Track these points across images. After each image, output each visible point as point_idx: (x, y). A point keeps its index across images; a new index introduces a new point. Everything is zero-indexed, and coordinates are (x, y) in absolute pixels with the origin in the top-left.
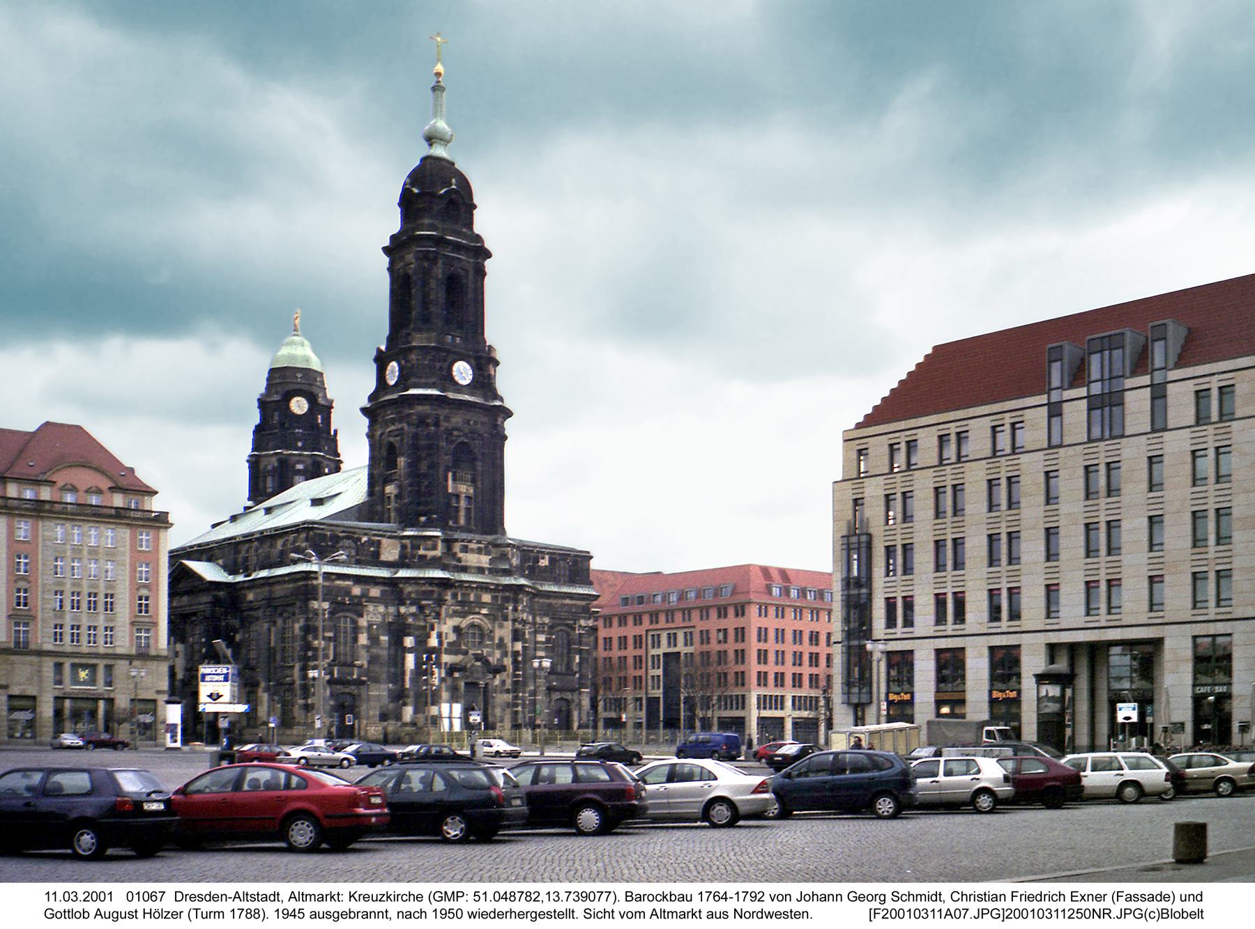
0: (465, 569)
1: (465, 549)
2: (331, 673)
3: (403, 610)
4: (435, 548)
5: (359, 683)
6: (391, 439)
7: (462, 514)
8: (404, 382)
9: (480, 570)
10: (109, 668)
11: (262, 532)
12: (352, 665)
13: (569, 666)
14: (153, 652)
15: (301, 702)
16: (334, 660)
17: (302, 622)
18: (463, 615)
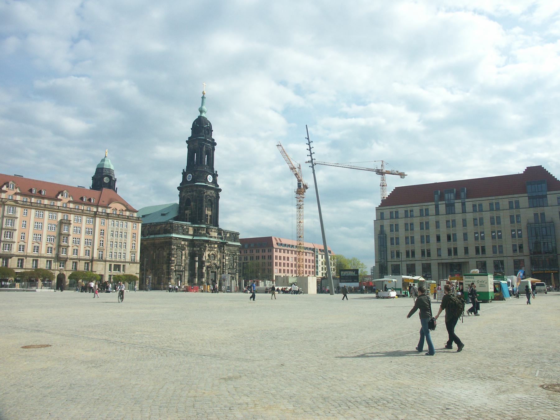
0: (211, 237)
1: (211, 231)
2: (176, 268)
3: (195, 249)
4: (204, 231)
5: (182, 271)
6: (189, 197)
7: (209, 220)
8: (194, 180)
9: (215, 237)
10: (124, 266)
11: (151, 224)
12: (181, 266)
13: (233, 267)
14: (136, 261)
15: (168, 277)
16: (177, 264)
17: (168, 252)
18: (210, 251)
